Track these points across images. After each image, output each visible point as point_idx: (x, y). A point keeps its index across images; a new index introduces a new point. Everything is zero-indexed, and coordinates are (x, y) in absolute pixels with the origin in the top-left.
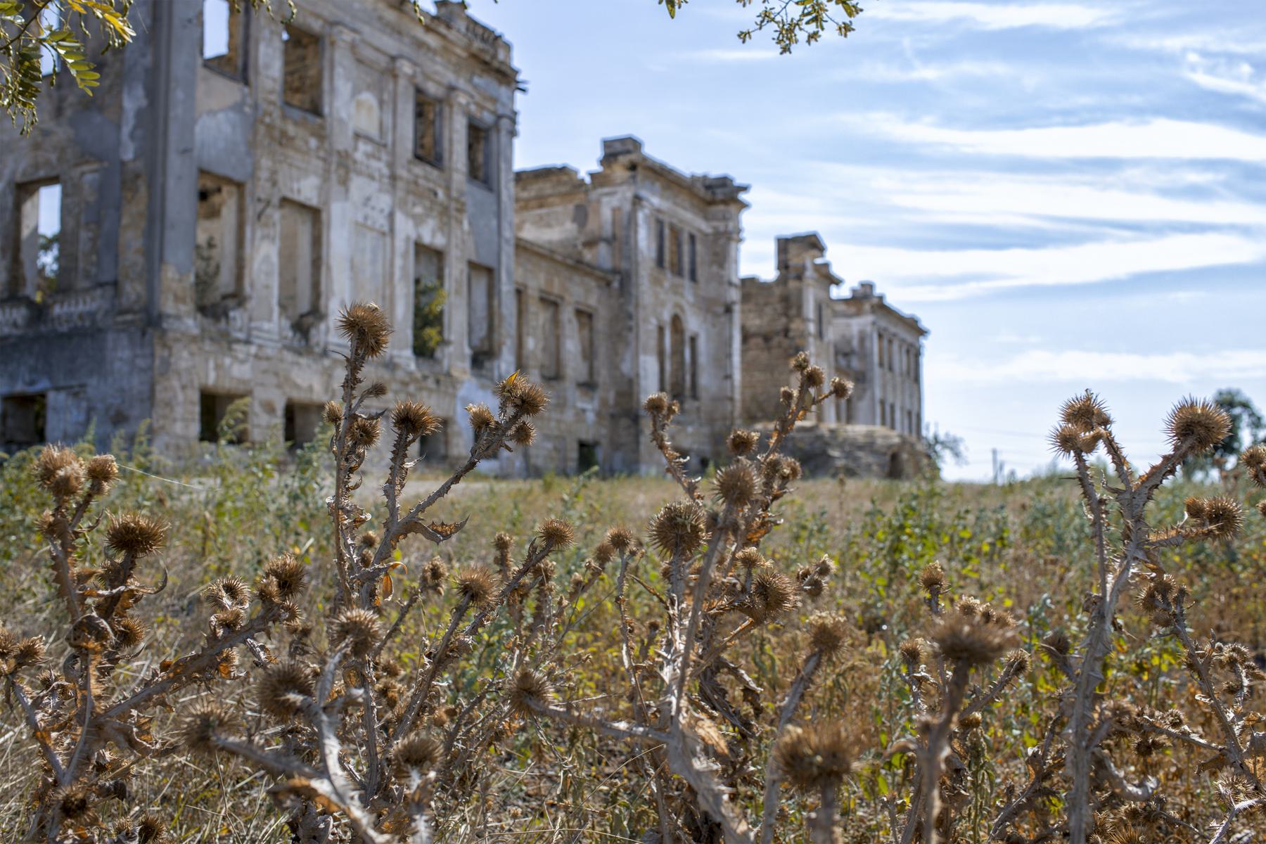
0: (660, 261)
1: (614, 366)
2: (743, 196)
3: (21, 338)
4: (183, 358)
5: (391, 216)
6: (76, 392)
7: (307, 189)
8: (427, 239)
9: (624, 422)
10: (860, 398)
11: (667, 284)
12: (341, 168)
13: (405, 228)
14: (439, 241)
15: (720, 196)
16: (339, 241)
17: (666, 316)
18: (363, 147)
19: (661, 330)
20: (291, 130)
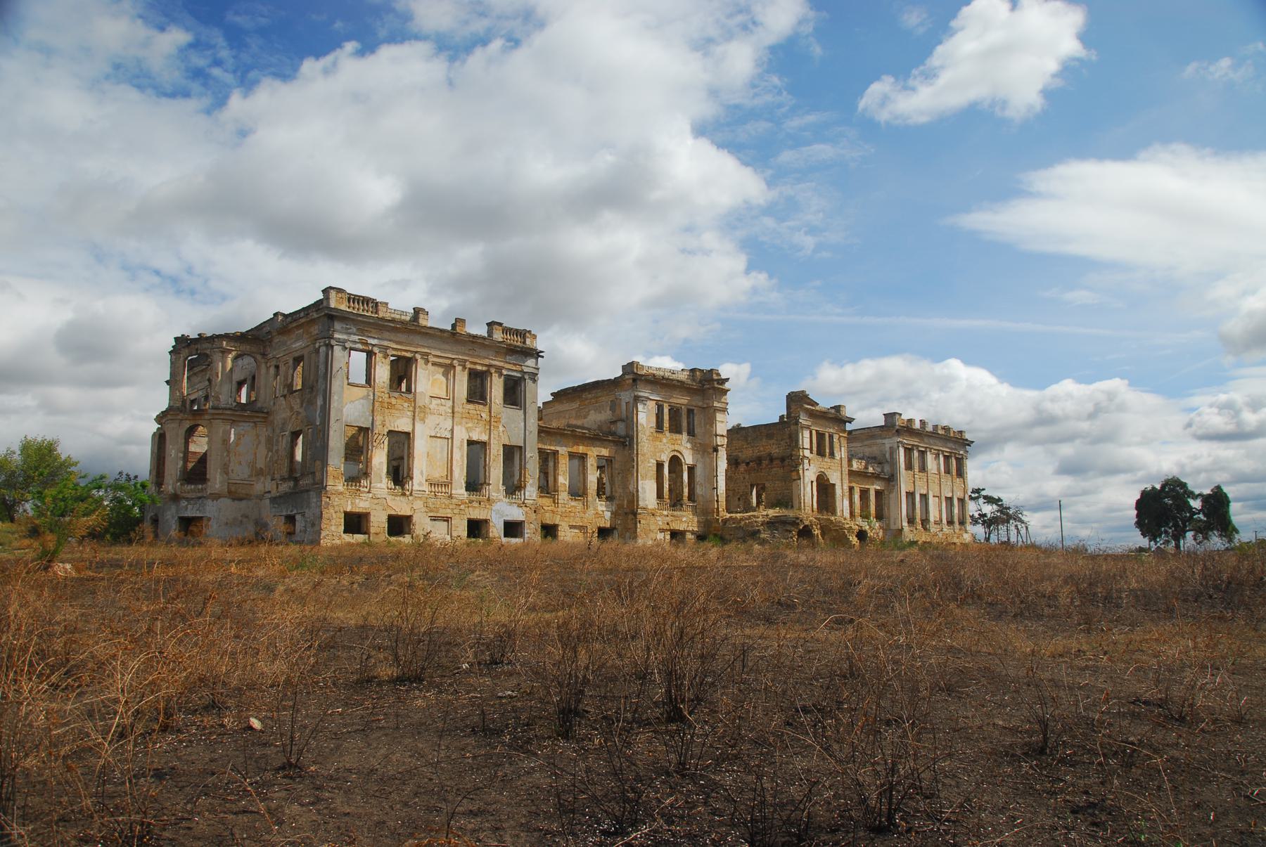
0: (659, 426)
1: (625, 487)
2: (727, 386)
3: (291, 494)
4: (336, 500)
5: (452, 431)
6: (303, 515)
7: (403, 425)
8: (475, 438)
9: (631, 516)
10: (890, 492)
11: (665, 440)
12: (418, 412)
13: (461, 435)
14: (484, 438)
15: (707, 386)
16: (420, 446)
17: (665, 458)
18: (435, 402)
19: (660, 466)
20: (393, 401)
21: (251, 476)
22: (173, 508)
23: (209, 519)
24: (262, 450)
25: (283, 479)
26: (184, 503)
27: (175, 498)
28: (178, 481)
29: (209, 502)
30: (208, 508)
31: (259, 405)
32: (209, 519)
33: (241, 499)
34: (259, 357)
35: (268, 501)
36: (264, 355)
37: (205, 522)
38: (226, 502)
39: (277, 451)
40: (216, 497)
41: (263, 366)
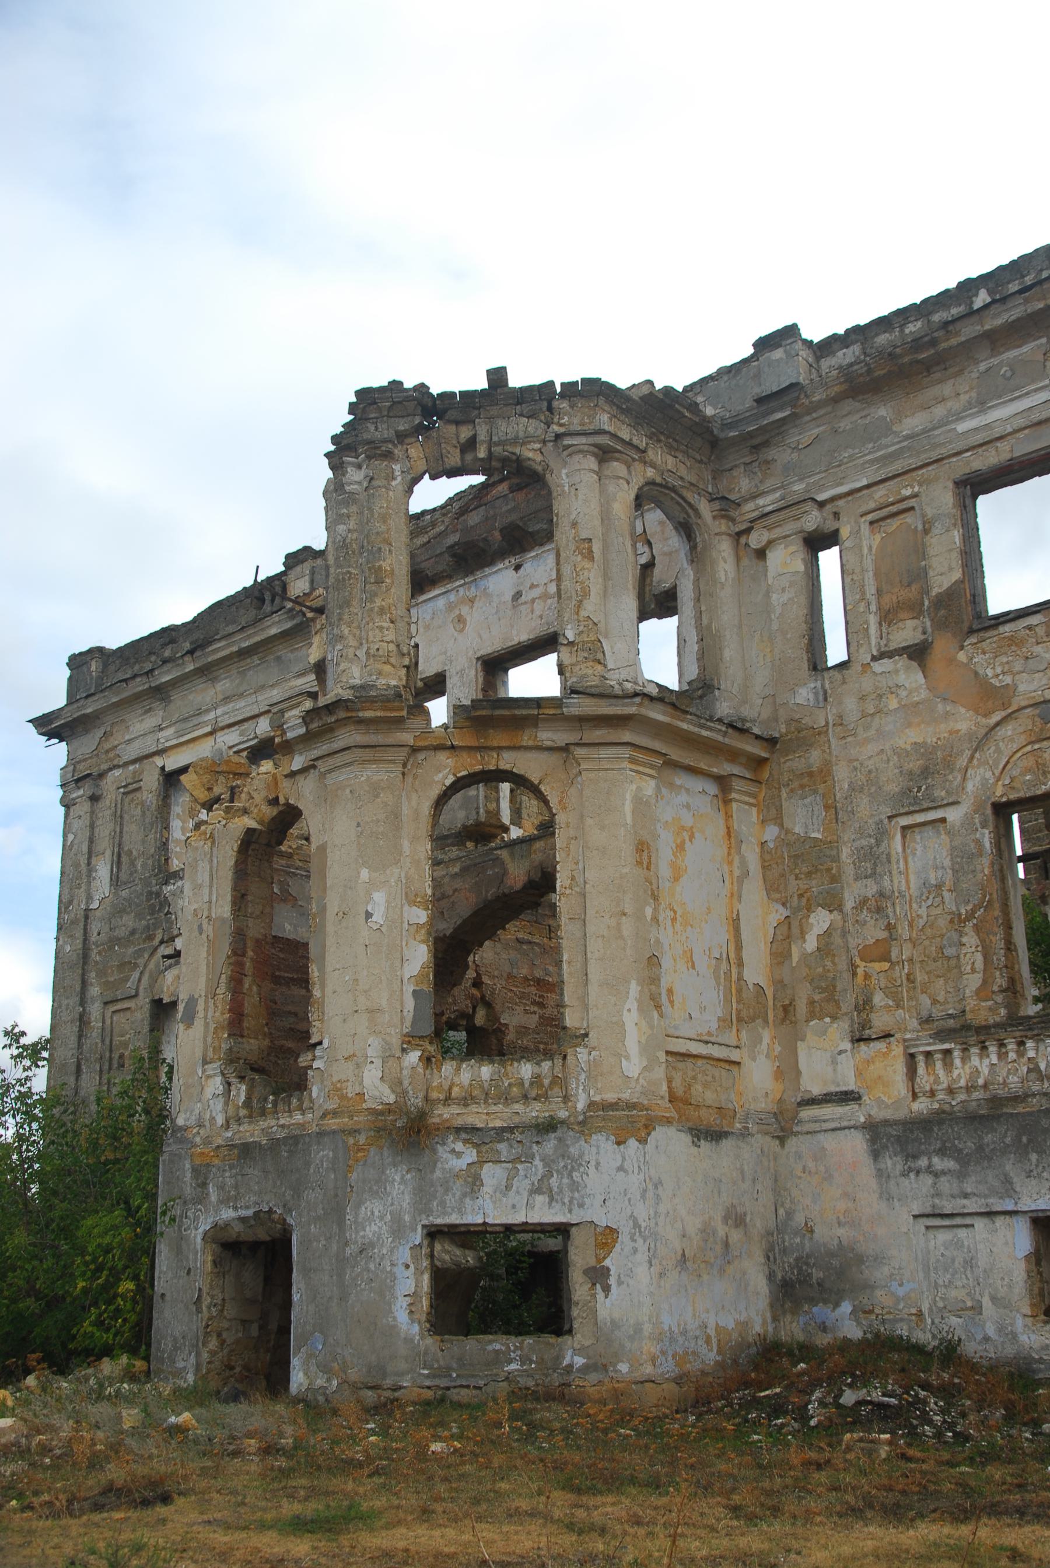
21: (725, 1022)
22: (400, 1184)
23: (607, 1238)
24: (761, 917)
25: (964, 1032)
26: (456, 1156)
27: (410, 1132)
28: (410, 1040)
29: (601, 1150)
30: (594, 1181)
31: (724, 708)
32: (607, 1238)
33: (716, 1136)
34: (705, 508)
35: (856, 1144)
36: (726, 506)
37: (580, 1257)
38: (670, 1143)
39: (878, 905)
40: (628, 1121)
41: (724, 548)
